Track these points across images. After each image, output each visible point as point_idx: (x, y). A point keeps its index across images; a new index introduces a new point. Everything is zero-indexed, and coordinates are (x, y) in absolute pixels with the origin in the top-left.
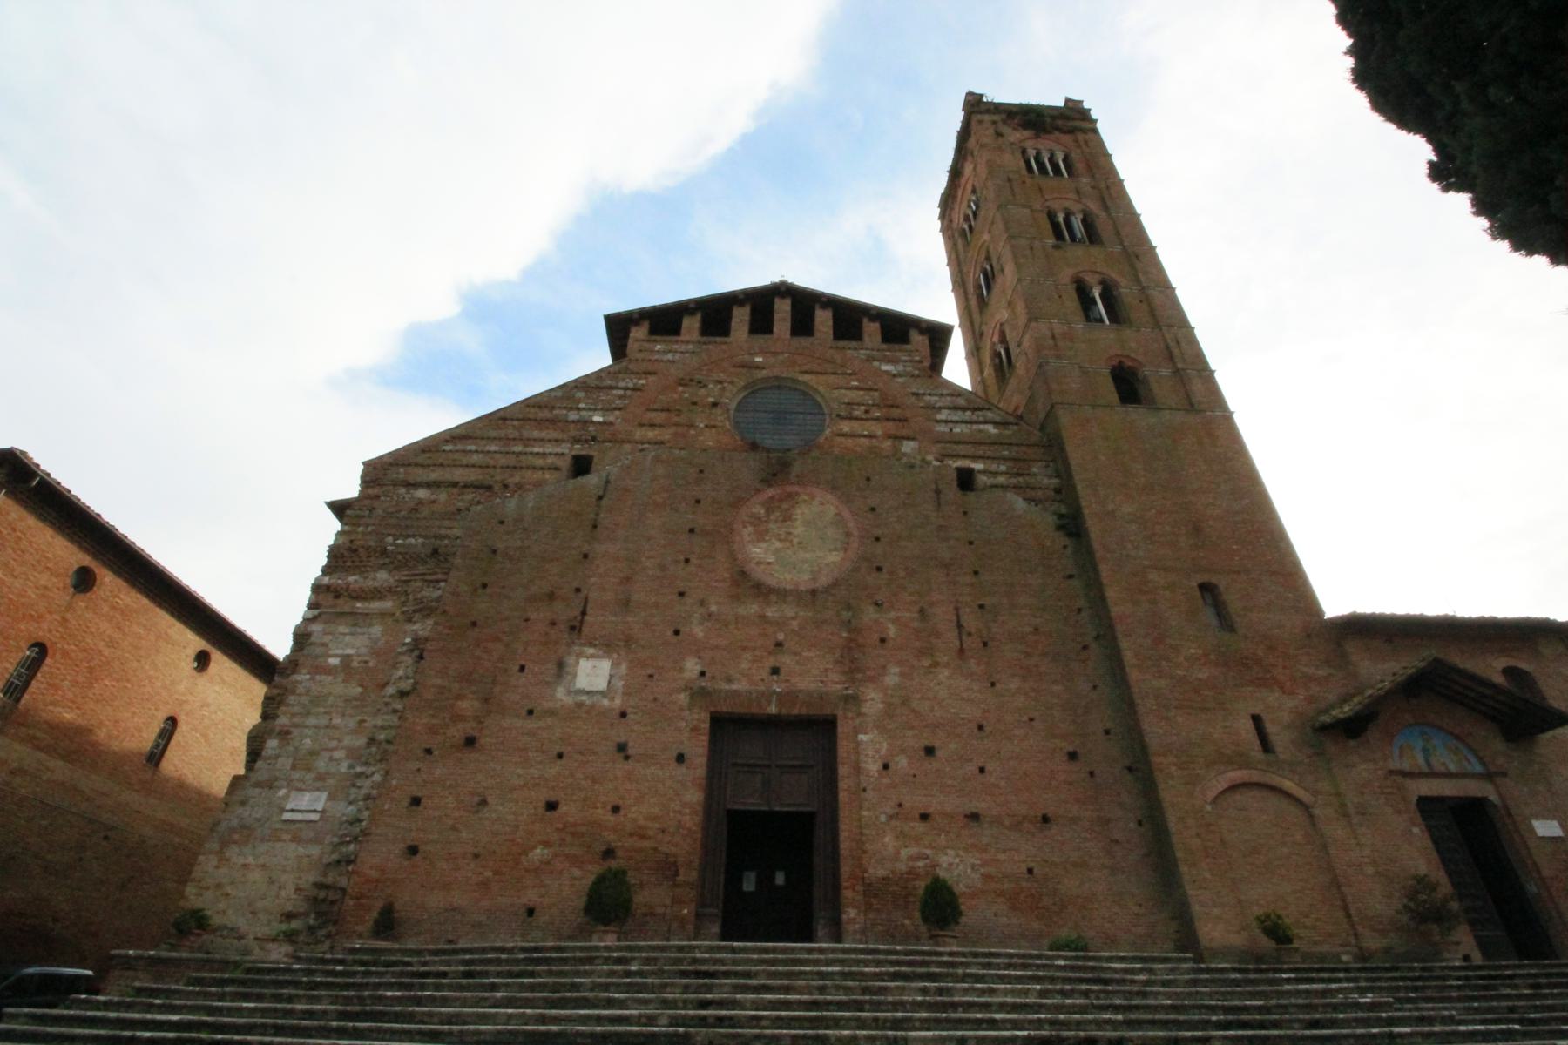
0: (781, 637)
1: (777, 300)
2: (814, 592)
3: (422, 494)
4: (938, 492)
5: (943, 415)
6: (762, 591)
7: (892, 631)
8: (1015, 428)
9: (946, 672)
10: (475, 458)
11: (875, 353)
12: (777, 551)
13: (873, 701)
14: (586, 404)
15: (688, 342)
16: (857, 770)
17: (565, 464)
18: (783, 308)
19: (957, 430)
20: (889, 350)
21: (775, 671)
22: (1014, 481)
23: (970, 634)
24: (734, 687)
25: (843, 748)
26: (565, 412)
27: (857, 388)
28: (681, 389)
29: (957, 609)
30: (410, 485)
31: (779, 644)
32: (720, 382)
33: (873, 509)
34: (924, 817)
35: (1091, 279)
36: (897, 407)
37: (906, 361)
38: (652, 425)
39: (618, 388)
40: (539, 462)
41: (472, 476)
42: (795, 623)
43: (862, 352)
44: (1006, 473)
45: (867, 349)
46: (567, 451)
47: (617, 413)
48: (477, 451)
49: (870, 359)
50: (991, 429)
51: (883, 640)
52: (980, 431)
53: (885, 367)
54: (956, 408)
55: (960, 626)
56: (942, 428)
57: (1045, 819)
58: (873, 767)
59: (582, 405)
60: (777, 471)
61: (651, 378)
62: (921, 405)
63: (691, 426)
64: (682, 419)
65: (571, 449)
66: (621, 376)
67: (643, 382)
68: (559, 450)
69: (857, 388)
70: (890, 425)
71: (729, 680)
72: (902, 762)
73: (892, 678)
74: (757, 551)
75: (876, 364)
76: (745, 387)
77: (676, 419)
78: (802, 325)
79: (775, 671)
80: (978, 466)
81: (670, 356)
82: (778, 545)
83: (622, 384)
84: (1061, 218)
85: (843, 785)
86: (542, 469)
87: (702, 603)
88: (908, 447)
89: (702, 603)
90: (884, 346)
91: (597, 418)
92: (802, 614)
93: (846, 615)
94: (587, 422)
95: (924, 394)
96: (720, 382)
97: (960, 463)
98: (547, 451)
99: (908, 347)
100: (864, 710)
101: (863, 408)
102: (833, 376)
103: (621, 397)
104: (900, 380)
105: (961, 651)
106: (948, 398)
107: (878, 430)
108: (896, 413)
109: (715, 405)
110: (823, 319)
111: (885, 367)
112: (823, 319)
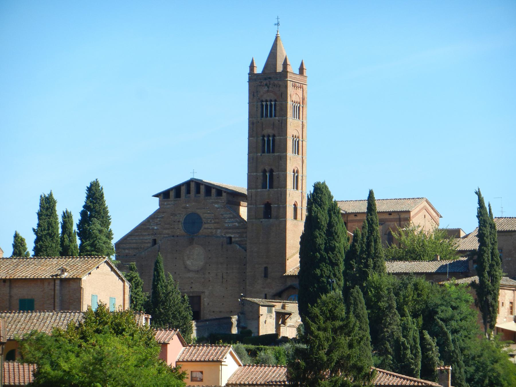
0: (192, 281)
1: (191, 183)
2: (198, 271)
3: (127, 251)
4: (222, 245)
5: (227, 221)
6: (189, 271)
7: (211, 279)
8: (242, 223)
9: (219, 287)
10: (134, 241)
11: (214, 200)
12: (192, 262)
13: (207, 293)
14: (153, 224)
15: (171, 201)
16: (204, 305)
17: (151, 241)
18: (193, 186)
19: (229, 225)
20: (217, 199)
21: (191, 288)
22: (239, 239)
23: (224, 279)
24: (185, 291)
25: (202, 301)
26: (149, 226)
27: (209, 213)
28: (171, 217)
29: (223, 274)
30: (124, 249)
31: (192, 283)
32: (180, 214)
33: (209, 251)
34: (214, 312)
35: (267, 168)
36: (217, 219)
37: (220, 203)
38: (166, 229)
39: (158, 218)
40: (146, 241)
41: (135, 246)
42: (194, 278)
43: (211, 200)
44: (238, 237)
45: (212, 199)
46: (151, 238)
47: (159, 226)
48: (134, 239)
49: (213, 203)
50: (237, 224)
51: (209, 281)
52: (234, 225)
53: (216, 206)
54: (230, 218)
55: (223, 277)
56: (226, 225)
57: (231, 312)
58: (206, 304)
59: (152, 224)
60: (191, 242)
61: (165, 214)
62: (223, 218)
63: (174, 228)
64: (172, 227)
65: (152, 237)
66: (158, 214)
67: (163, 215)
68: (149, 238)
69: (209, 213)
70: (215, 225)
71: (184, 290)
72: (211, 303)
73: (210, 288)
74: (188, 263)
75: (214, 204)
76: (185, 215)
77: (171, 227)
78: (198, 191)
79: (191, 288)
80: (232, 236)
81: (168, 206)
82: (192, 261)
83: (159, 217)
84: (266, 139)
85: (202, 307)
86: (147, 243)
87: (179, 275)
88: (219, 231)
89: (179, 275)
90: (216, 198)
91: (155, 228)
92: (196, 276)
93: (203, 276)
94: (153, 229)
95: (224, 214)
96: (180, 214)
97: (228, 235)
98: (147, 238)
99: (221, 197)
100: (205, 294)
101: (210, 220)
102: (204, 210)
103: (160, 221)
104: (218, 210)
105: (222, 282)
106: (229, 215)
107: (212, 226)
108: (217, 220)
109: (179, 222)
110: (202, 188)
111: (216, 206)
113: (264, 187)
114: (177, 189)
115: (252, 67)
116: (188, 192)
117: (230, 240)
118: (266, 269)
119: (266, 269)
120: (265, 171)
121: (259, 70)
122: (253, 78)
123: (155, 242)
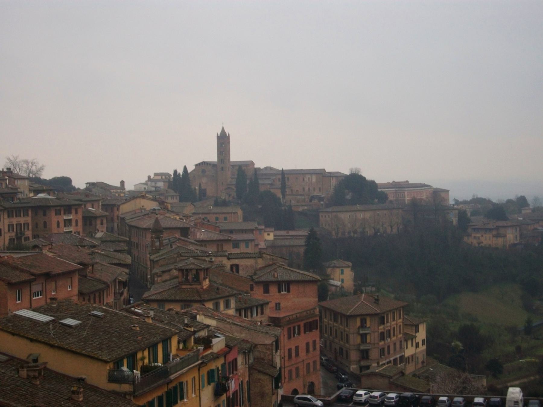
110: (206, 164)
112: (206, 164)
113: (221, 163)
114: (200, 164)
115: (218, 134)
116: (202, 164)
117: (213, 176)
118: (222, 183)
119: (222, 183)
120: (221, 160)
121: (219, 135)
122: (218, 136)
123: (194, 176)
